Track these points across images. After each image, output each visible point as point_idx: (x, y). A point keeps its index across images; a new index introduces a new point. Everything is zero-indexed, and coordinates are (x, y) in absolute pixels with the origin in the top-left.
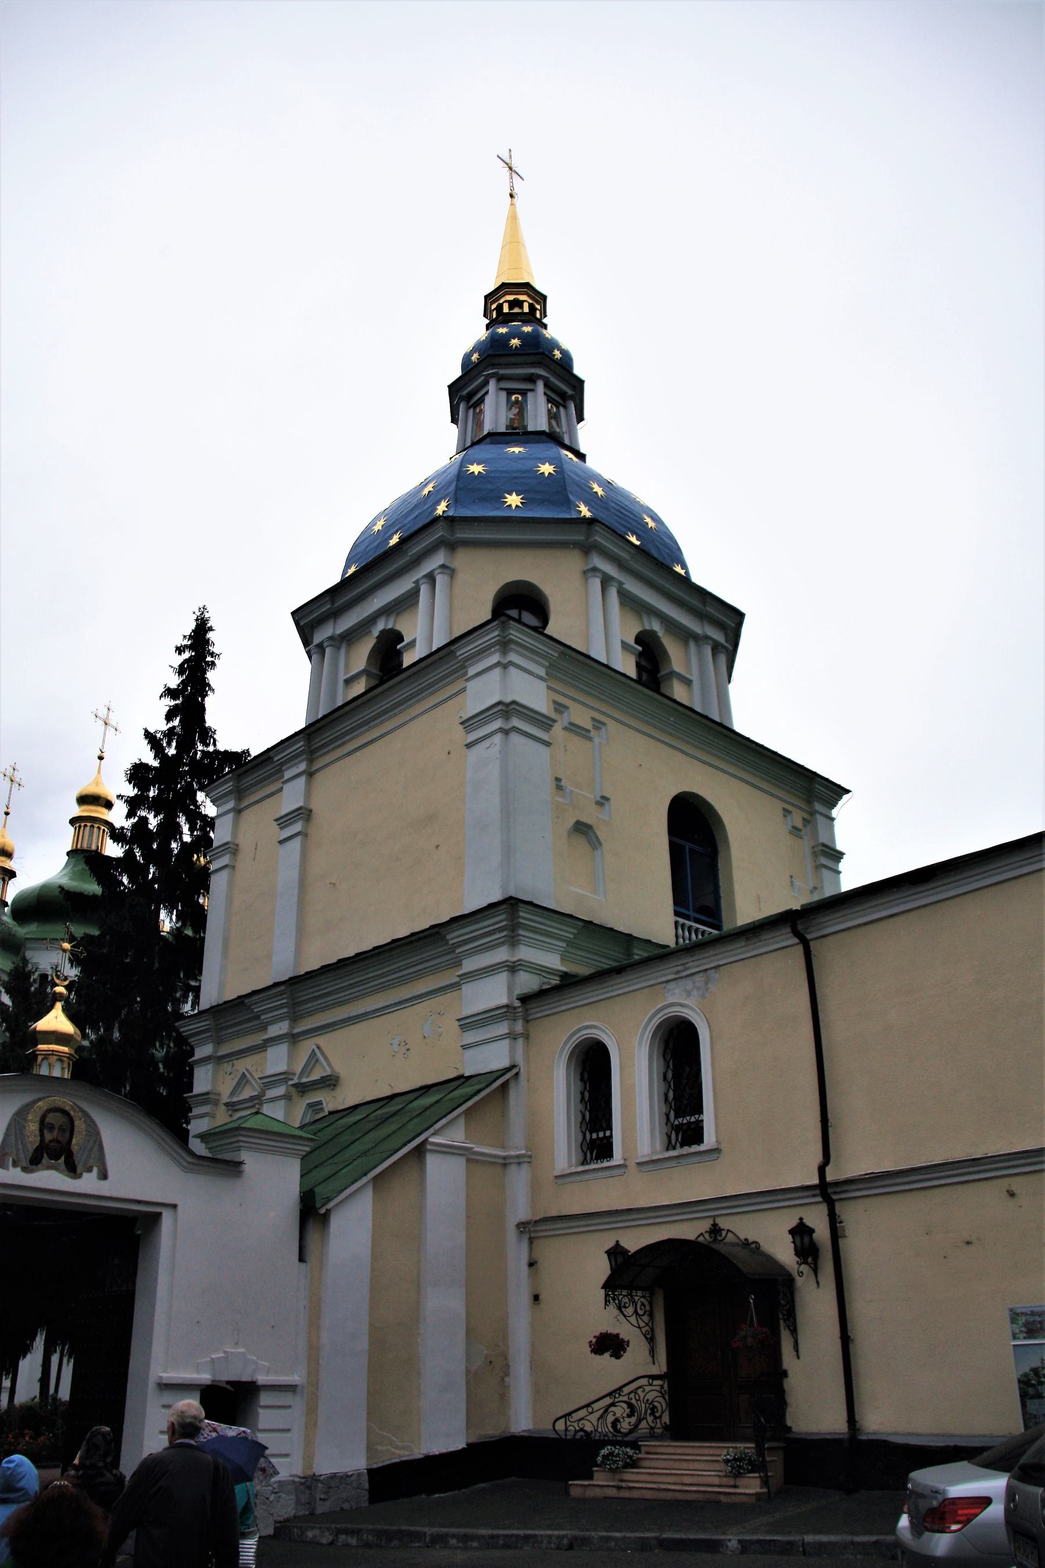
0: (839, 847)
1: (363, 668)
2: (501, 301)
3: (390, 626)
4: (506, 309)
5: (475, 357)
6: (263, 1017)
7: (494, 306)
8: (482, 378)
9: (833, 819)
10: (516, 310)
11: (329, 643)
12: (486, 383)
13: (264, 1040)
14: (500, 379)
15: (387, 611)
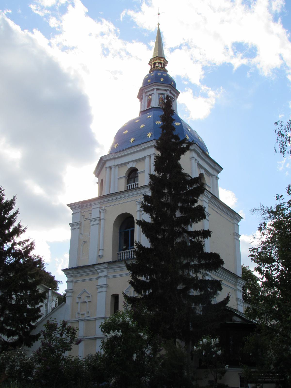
0: (240, 234)
1: (124, 176)
2: (156, 62)
3: (134, 166)
4: (157, 65)
5: (149, 81)
6: (98, 271)
7: (153, 63)
8: (152, 88)
9: (239, 226)
10: (160, 66)
11: (113, 166)
12: (153, 90)
13: (98, 277)
14: (158, 89)
15: (134, 161)
